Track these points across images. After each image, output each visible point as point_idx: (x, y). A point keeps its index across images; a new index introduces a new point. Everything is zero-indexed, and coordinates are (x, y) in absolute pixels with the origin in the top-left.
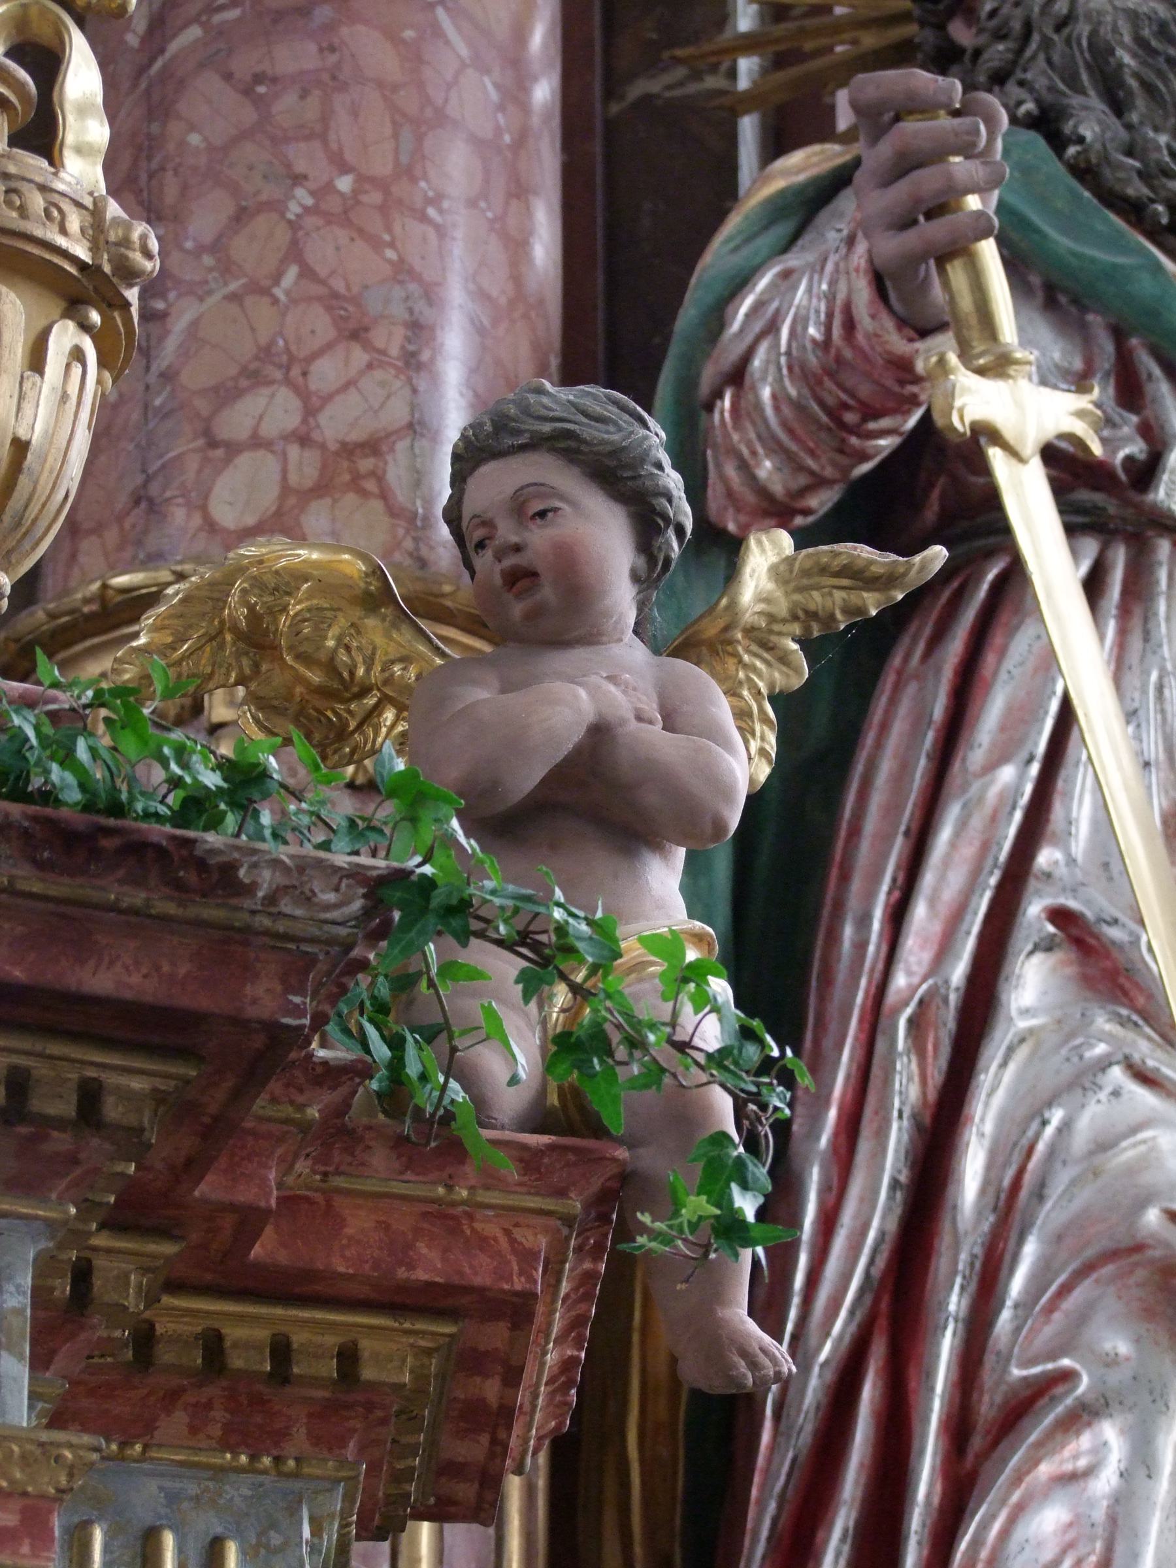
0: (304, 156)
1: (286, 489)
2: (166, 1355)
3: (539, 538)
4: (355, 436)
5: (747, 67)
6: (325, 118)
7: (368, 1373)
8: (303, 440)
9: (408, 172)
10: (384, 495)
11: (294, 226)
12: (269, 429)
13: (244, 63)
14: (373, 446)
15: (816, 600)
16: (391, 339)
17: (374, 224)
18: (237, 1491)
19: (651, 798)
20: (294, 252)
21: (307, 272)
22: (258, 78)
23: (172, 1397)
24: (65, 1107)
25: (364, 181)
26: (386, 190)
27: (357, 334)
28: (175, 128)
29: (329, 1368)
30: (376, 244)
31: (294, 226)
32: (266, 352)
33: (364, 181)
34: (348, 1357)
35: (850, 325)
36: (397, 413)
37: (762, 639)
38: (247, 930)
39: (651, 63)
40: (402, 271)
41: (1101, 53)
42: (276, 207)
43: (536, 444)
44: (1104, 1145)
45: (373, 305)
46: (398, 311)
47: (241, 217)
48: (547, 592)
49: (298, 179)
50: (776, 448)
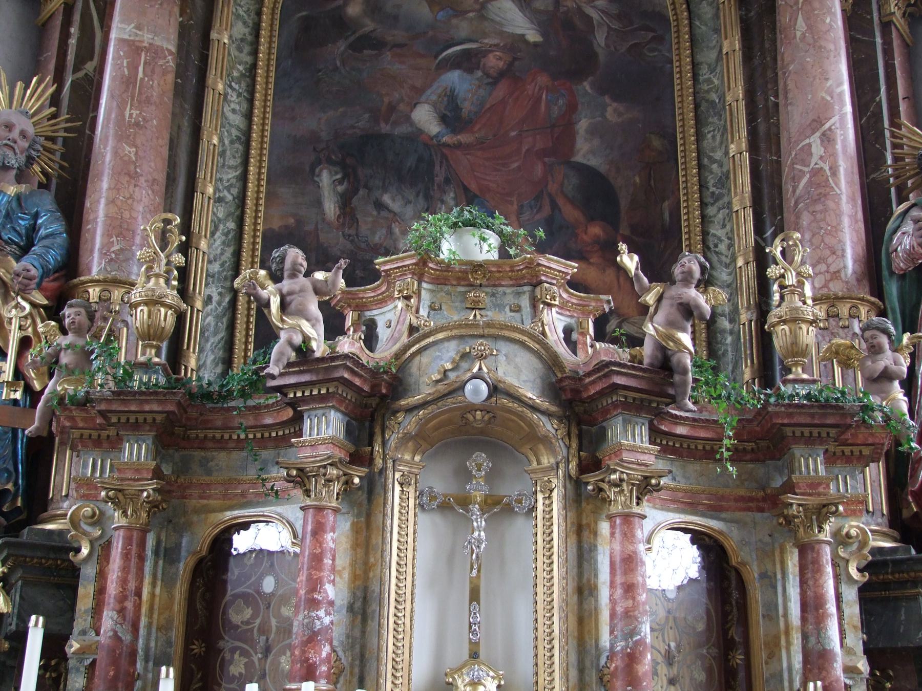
0: (822, 224)
1: (826, 280)
2: (837, 454)
3: (875, 341)
4: (836, 270)
5: (891, 180)
6: (825, 217)
7: (864, 453)
8: (828, 272)
10: (841, 279)
11: (822, 236)
12: (822, 271)
13: (811, 209)
14: (839, 271)
15: (913, 341)
16: (839, 253)
17: (835, 235)
18: (848, 469)
20: (823, 241)
21: (825, 244)
22: (814, 212)
23: (838, 459)
24: (825, 435)
25: (832, 227)
26: (835, 227)
27: (834, 253)
28: (801, 221)
29: (858, 453)
30: (835, 237)
31: (822, 236)
32: (820, 258)
33: (832, 227)
34: (861, 452)
35: (914, 248)
36: (842, 265)
37: (907, 347)
38: (846, 414)
40: (840, 241)
42: (819, 233)
43: (873, 328)
45: (836, 247)
46: (840, 248)
47: (814, 235)
48: (877, 348)
49: (822, 228)
50: (903, 262)
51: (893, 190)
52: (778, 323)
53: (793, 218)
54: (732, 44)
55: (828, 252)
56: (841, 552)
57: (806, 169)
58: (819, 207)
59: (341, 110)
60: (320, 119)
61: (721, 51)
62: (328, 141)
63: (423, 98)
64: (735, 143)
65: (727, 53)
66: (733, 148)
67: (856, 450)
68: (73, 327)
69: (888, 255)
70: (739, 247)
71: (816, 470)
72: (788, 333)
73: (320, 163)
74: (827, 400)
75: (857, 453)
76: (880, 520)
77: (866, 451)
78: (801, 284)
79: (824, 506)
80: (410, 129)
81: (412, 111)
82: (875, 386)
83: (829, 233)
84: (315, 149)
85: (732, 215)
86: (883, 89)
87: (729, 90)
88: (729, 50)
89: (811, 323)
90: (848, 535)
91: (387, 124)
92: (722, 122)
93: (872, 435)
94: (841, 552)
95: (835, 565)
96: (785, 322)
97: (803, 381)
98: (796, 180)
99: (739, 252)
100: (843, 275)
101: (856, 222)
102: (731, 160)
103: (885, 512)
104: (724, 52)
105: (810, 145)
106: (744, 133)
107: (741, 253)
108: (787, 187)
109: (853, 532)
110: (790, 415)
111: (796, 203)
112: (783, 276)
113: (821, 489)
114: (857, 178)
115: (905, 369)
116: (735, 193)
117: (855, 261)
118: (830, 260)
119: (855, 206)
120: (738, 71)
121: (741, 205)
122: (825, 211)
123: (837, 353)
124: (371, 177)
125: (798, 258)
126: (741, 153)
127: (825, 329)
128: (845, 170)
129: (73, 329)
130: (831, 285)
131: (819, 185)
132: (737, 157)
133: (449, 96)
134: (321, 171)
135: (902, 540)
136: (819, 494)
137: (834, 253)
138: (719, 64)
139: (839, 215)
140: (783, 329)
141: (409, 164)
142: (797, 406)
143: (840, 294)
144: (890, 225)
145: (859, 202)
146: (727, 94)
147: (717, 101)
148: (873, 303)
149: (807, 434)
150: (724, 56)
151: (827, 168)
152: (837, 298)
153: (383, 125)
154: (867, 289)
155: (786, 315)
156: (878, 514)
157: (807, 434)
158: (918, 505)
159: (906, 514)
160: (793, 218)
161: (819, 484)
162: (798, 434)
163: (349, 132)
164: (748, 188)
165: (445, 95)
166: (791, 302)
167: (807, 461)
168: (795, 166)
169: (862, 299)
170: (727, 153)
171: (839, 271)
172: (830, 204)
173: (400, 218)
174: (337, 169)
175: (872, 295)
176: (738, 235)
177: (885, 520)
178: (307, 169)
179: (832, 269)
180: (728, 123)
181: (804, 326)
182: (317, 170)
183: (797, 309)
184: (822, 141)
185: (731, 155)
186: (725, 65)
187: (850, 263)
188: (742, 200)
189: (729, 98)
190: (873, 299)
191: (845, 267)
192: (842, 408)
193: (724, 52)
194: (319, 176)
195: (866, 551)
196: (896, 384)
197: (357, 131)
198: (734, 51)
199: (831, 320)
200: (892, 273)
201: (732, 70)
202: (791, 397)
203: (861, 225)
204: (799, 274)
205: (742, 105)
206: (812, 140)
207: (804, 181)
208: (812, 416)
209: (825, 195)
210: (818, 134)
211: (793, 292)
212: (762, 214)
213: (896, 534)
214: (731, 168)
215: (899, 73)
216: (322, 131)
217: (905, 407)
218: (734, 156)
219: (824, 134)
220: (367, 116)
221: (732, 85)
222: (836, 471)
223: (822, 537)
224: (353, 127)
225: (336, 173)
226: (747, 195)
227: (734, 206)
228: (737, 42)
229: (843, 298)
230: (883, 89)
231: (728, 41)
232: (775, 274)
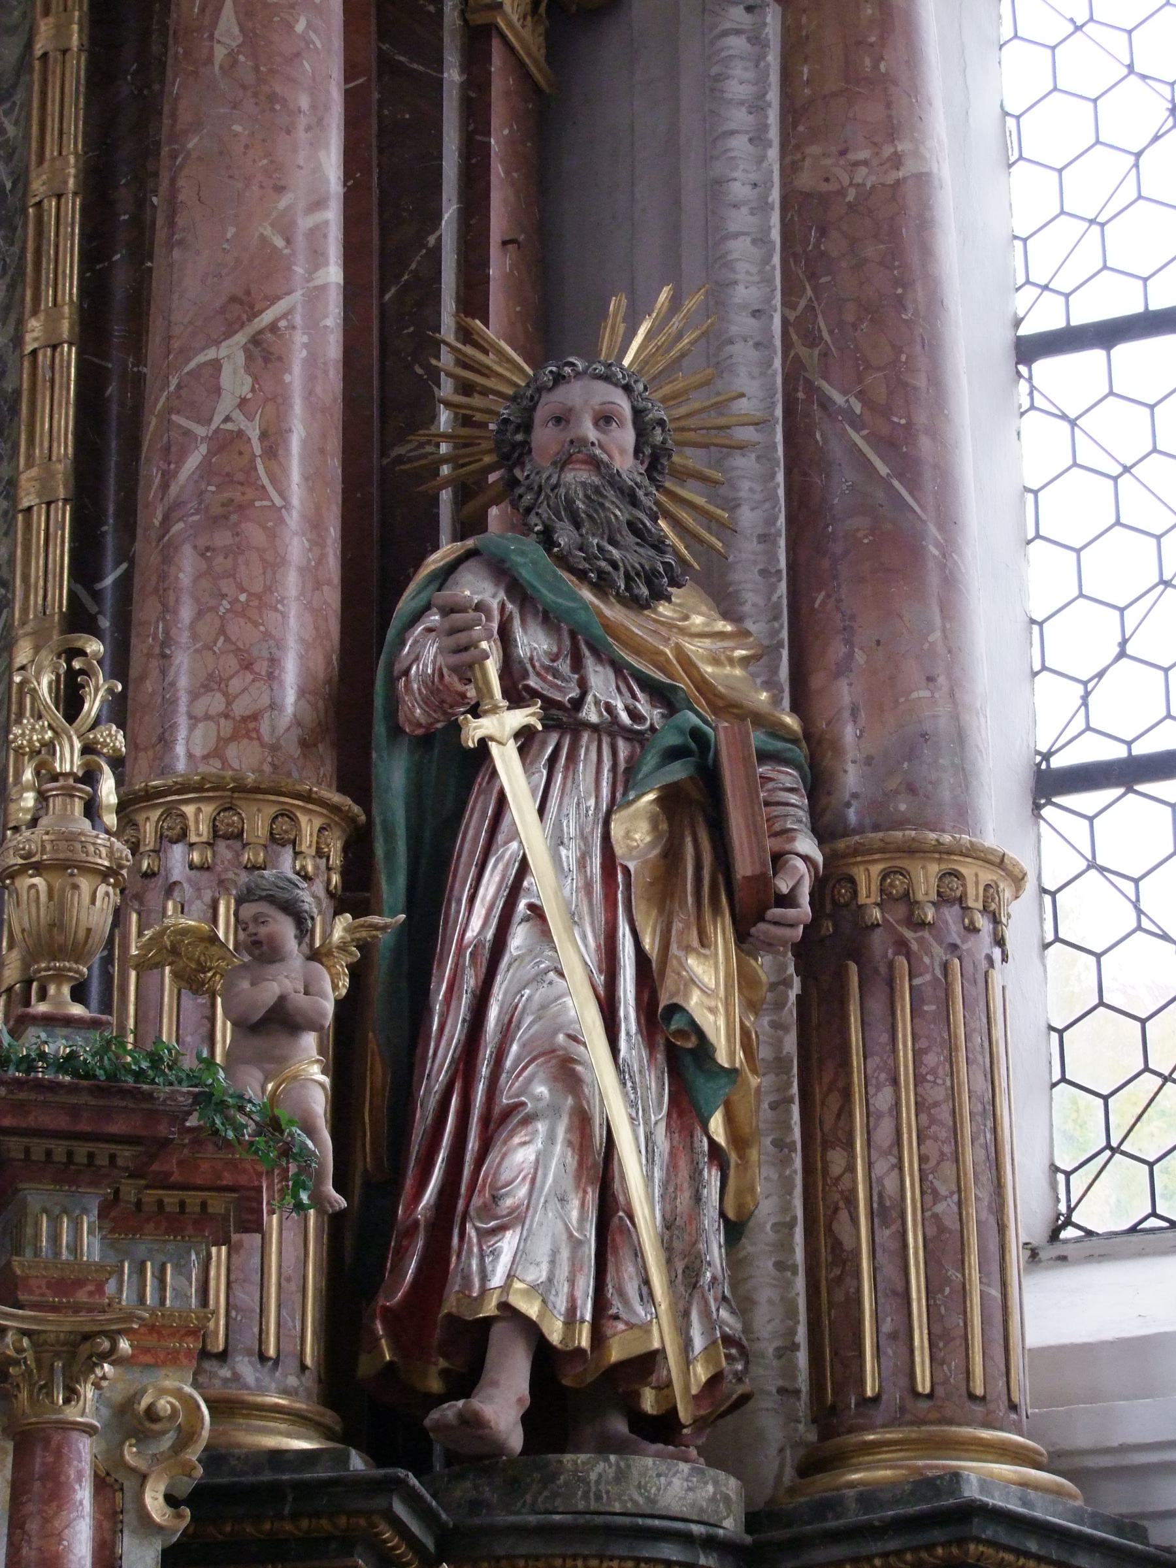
0: (227, 586)
1: (219, 738)
2: (145, 1208)
3: (263, 931)
4: (247, 713)
6: (235, 566)
7: (210, 1210)
8: (227, 716)
9: (269, 589)
10: (259, 738)
11: (222, 618)
12: (212, 712)
13: (202, 542)
14: (255, 717)
15: (358, 935)
16: (262, 667)
17: (256, 617)
18: (170, 1247)
19: (299, 1019)
20: (222, 631)
21: (228, 640)
22: (208, 549)
23: (148, 1220)
24: (106, 1162)
25: (250, 595)
26: (260, 598)
27: (247, 666)
28: (173, 570)
29: (198, 1209)
30: (256, 624)
31: (222, 618)
32: (211, 676)
33: (250, 595)
34: (204, 1205)
35: (441, 676)
36: (265, 700)
37: (343, 947)
38: (157, 1111)
39: (401, 439)
40: (267, 635)
41: (570, 502)
42: (214, 609)
43: (261, 898)
44: (544, 1007)
45: (255, 653)
46: (265, 654)
47: (200, 614)
48: (265, 948)
49: (224, 596)
50: (421, 707)
51: (446, 496)
52: (23, 870)
53: (155, 559)
54: (61, 31)
55: (232, 663)
56: (130, 1454)
57: (200, 431)
58: (223, 538)
61: (29, 45)
64: (42, 316)
65: (45, 55)
66: (35, 329)
67: (193, 1199)
69: (391, 681)
70: (25, 610)
71: (75, 1248)
72: (43, 897)
74: (112, 1077)
75: (193, 1207)
76: (292, 1381)
77: (218, 1204)
78: (90, 777)
79: (87, 1337)
82: (258, 1043)
83: (242, 612)
85: (14, 518)
86: (450, 212)
87: (41, 160)
88: (50, 47)
89: (105, 875)
90: (151, 1414)
92: (16, 249)
93: (233, 1165)
94: (130, 1454)
95: (103, 1485)
96: (38, 868)
97: (69, 1022)
98: (173, 454)
99: (24, 623)
100: (265, 727)
101: (318, 585)
102: (26, 364)
103: (309, 1361)
104: (38, 52)
105: (216, 365)
106: (70, 288)
107: (28, 628)
108: (152, 472)
109: (164, 1405)
110: (20, 1108)
111: (167, 521)
112: (50, 746)
113: (82, 1296)
114: (334, 465)
115: (329, 1007)
116: (30, 457)
117: (302, 693)
118: (235, 685)
119: (318, 542)
120: (70, 111)
121: (39, 496)
122: (235, 551)
123: (174, 951)
125: (93, 706)
126: (54, 347)
127: (203, 868)
128: (305, 443)
130: (232, 752)
131: (228, 480)
132: (43, 358)
135: (349, 1437)
136: (76, 1309)
137: (247, 666)
138: (24, 78)
139: (274, 564)
140: (33, 886)
142: (39, 1085)
143: (251, 778)
144: (406, 603)
145: (334, 532)
146: (33, 175)
147: (9, 185)
148: (335, 809)
149: (59, 1154)
150: (37, 65)
151: (254, 434)
152: (243, 790)
154: (328, 768)
155: (43, 852)
156: (291, 1364)
157: (59, 1154)
158: (395, 1346)
159: (365, 1367)
160: (155, 559)
161: (79, 1283)
162: (38, 1155)
164: (65, 448)
166: (65, 817)
167: (55, 1223)
168: (174, 417)
169: (307, 797)
170: (18, 340)
171: (255, 717)
172: (254, 533)
175: (341, 789)
176: (26, 578)
177: (309, 1380)
179: (241, 708)
180: (29, 256)
181: (85, 884)
183: (71, 838)
184: (249, 357)
185: (29, 348)
186: (36, 87)
187: (290, 698)
188: (45, 482)
189: (38, 186)
190: (337, 798)
191: (274, 706)
192: (149, 1097)
193: (38, 52)
195: (193, 1454)
196: (310, 1041)
198: (65, 52)
199: (222, 845)
200: (396, 731)
201: (53, 108)
202: (28, 1064)
203: (332, 597)
204: (87, 750)
205: (73, 207)
206: (223, 351)
207: (193, 461)
208: (74, 1112)
209: (241, 507)
210: (241, 338)
211: (69, 794)
212: (100, 521)
213: (329, 1417)
214: (25, 386)
215: (498, 170)
217: (319, 1103)
218: (34, 352)
219: (256, 340)
221: (51, 150)
222: (141, 1249)
223: (72, 1413)
226: (60, 467)
227: (22, 493)
228: (75, 27)
229: (257, 790)
230: (450, 212)
231: (51, 20)
232: (30, 741)
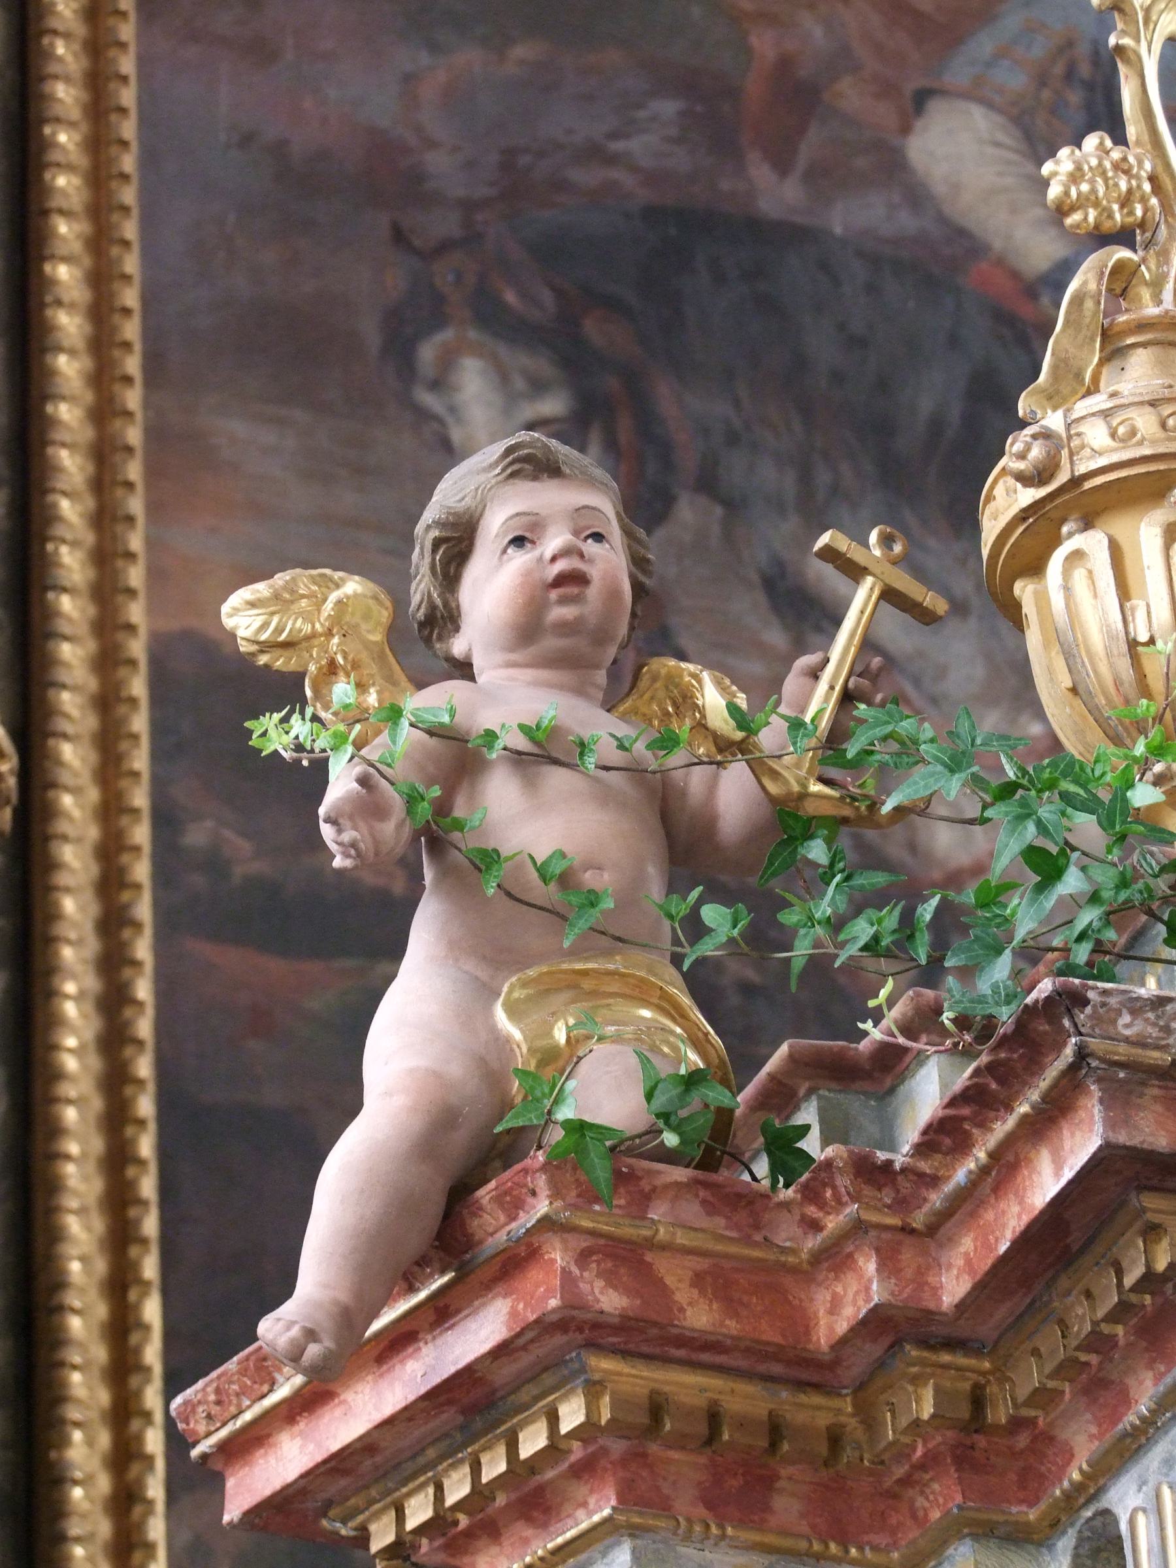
59: (520, 51)
60: (409, 79)
62: (468, 206)
63: (958, 72)
68: (560, 613)
73: (438, 318)
80: (907, 222)
81: (906, 129)
84: (399, 236)
91: (782, 167)
124: (733, 439)
129: (566, 628)
133: (1089, 86)
134: (448, 360)
141: (926, 405)
153: (760, 172)
163: (585, 177)
165: (1070, 75)
173: (917, 682)
174: (542, 365)
178: (371, 332)
182: (427, 353)
194: (437, 385)
197: (617, 174)
216: (432, 144)
220: (668, 108)
224: (594, 153)
225: (538, 387)
